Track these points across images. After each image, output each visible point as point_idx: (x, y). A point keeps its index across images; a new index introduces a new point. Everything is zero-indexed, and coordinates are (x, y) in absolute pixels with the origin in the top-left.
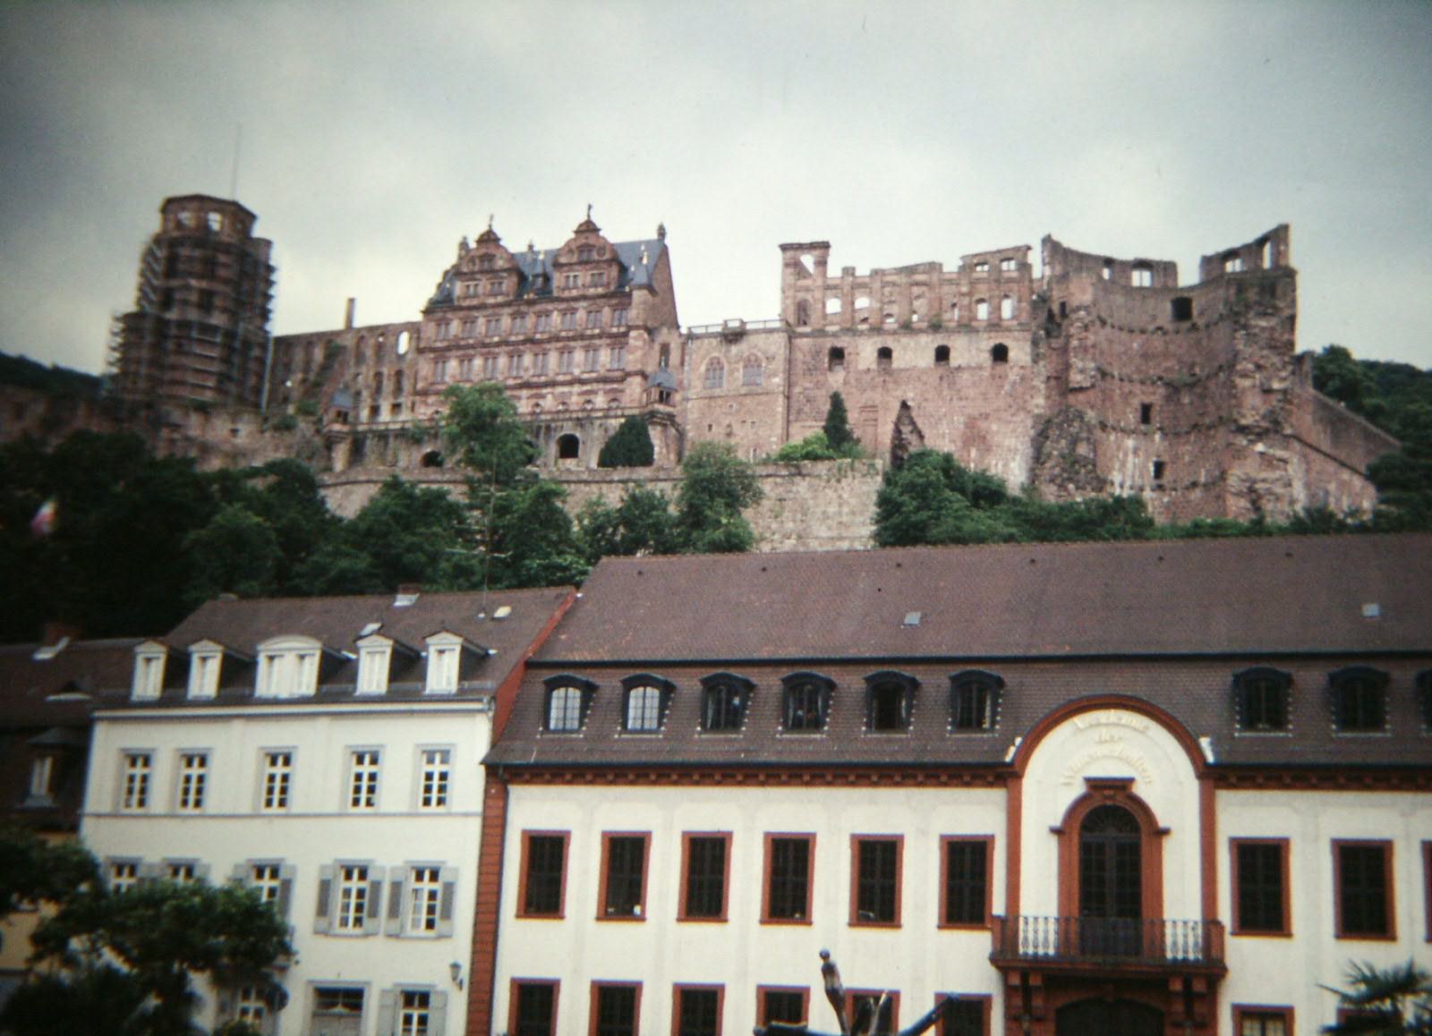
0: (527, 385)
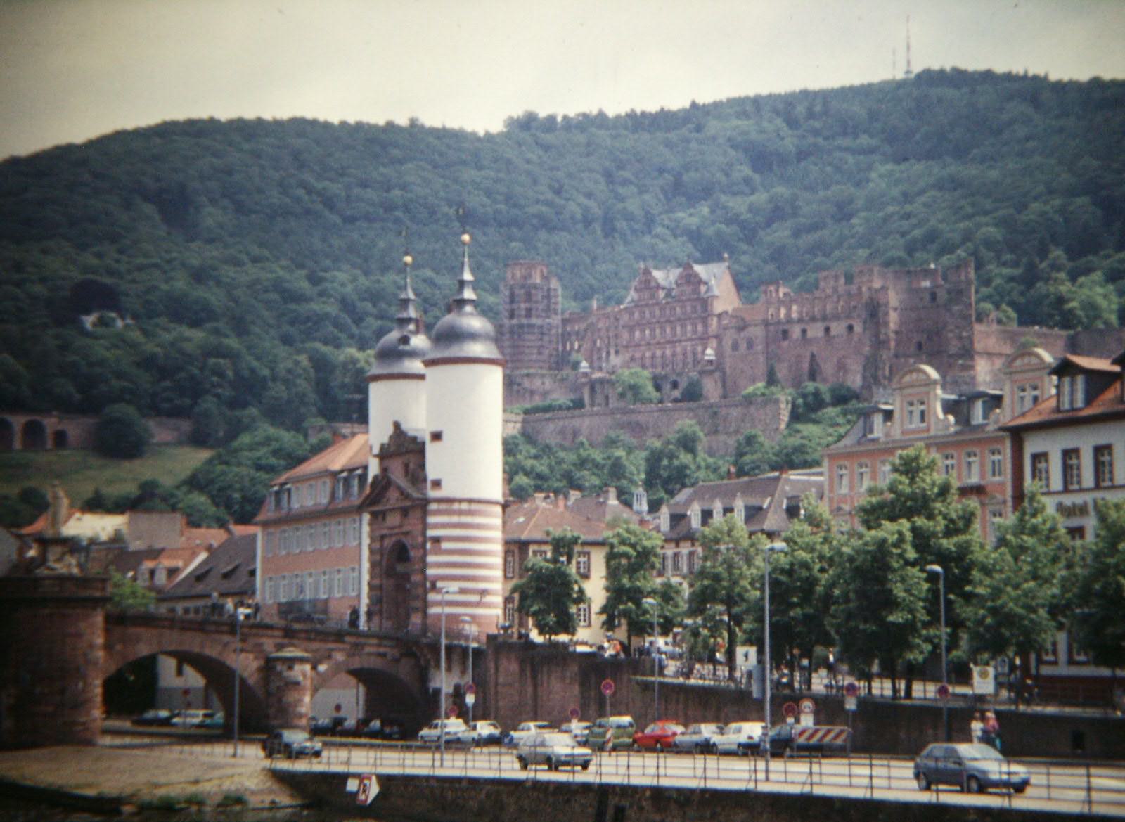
0: (669, 342)
